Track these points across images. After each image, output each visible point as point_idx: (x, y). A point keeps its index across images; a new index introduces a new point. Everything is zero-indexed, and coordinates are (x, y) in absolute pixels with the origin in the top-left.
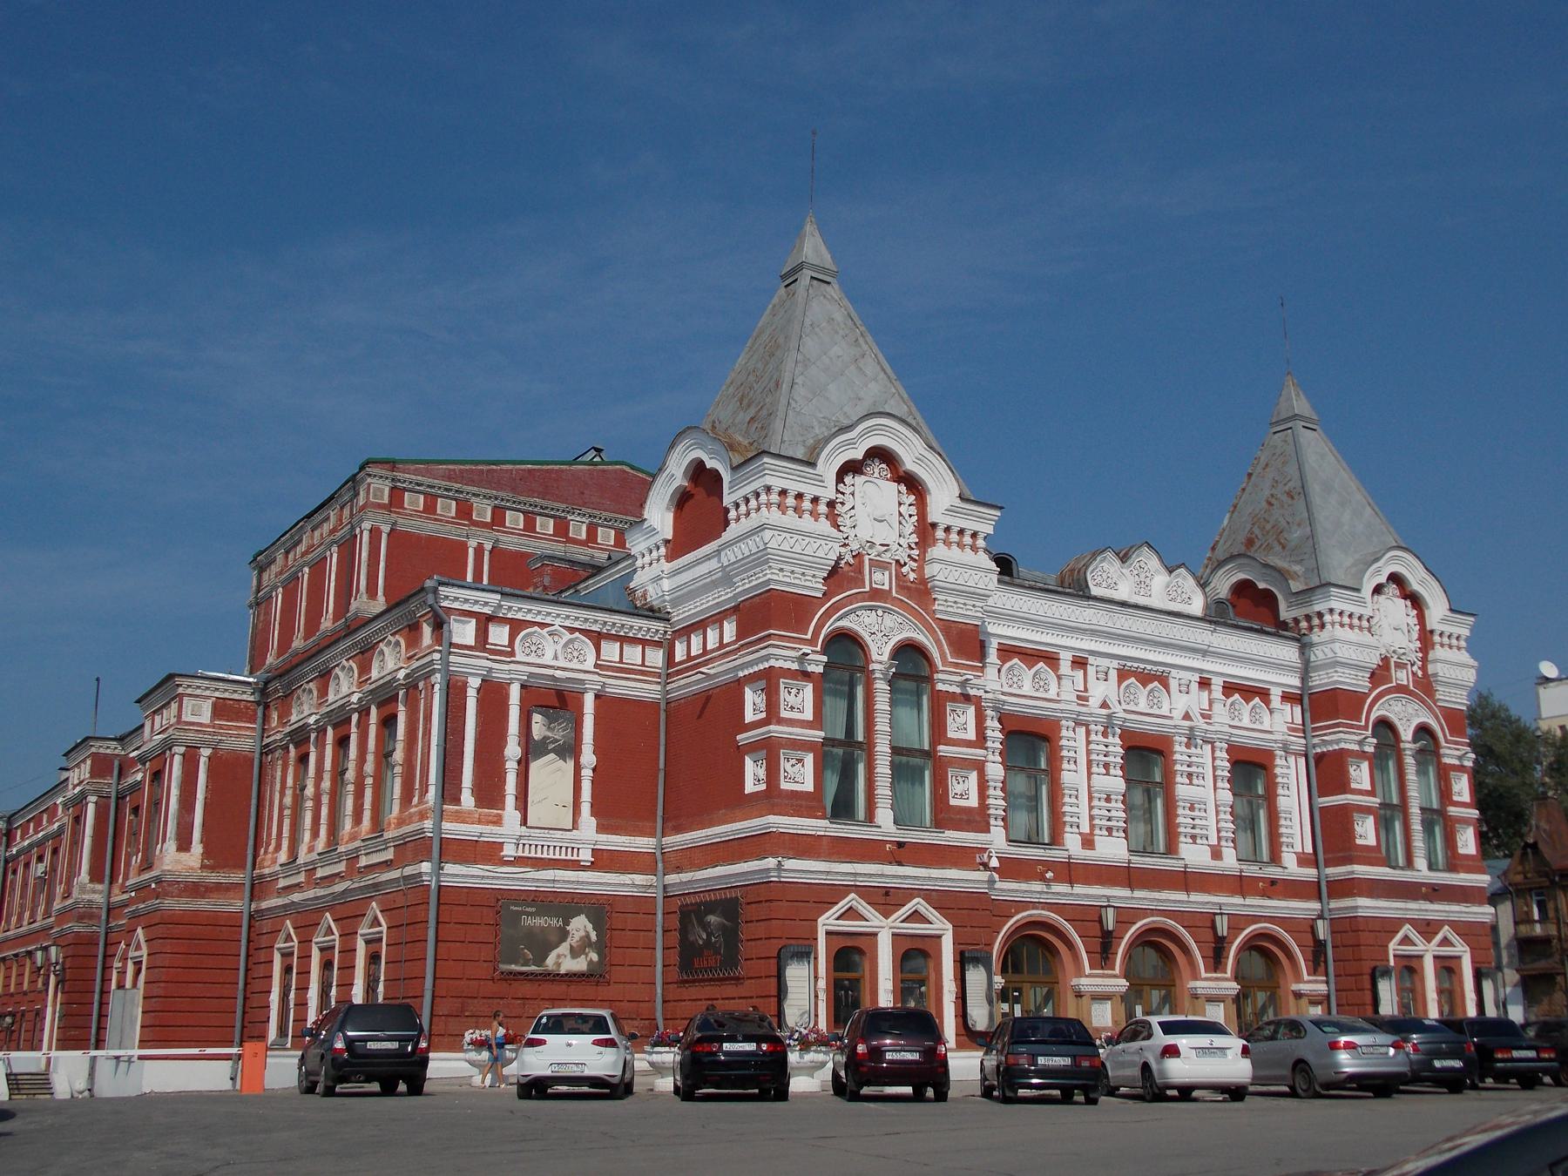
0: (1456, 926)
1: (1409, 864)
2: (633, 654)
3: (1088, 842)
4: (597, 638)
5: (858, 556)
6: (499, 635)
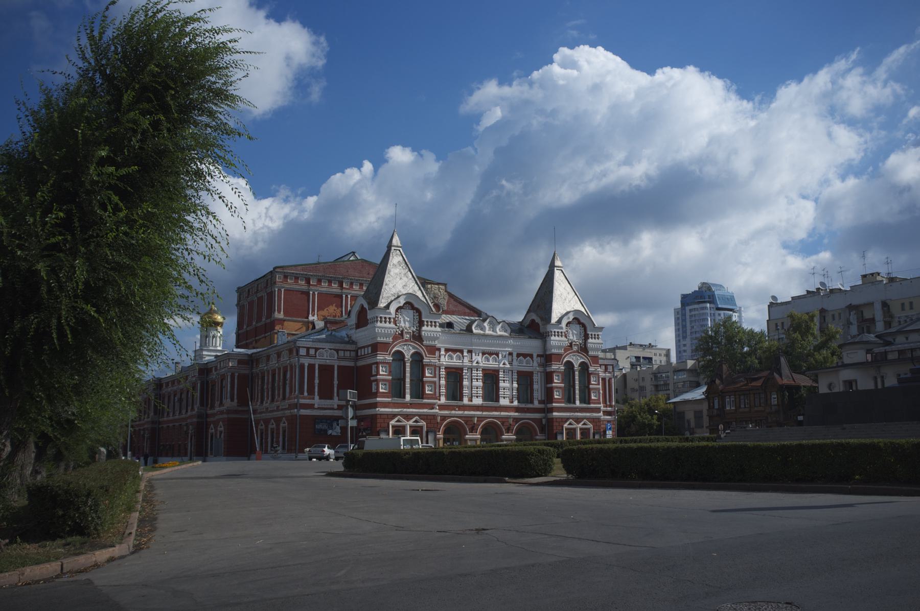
0: (588, 419)
1: (574, 403)
2: (347, 354)
4: (337, 351)
5: (402, 331)
6: (312, 352)
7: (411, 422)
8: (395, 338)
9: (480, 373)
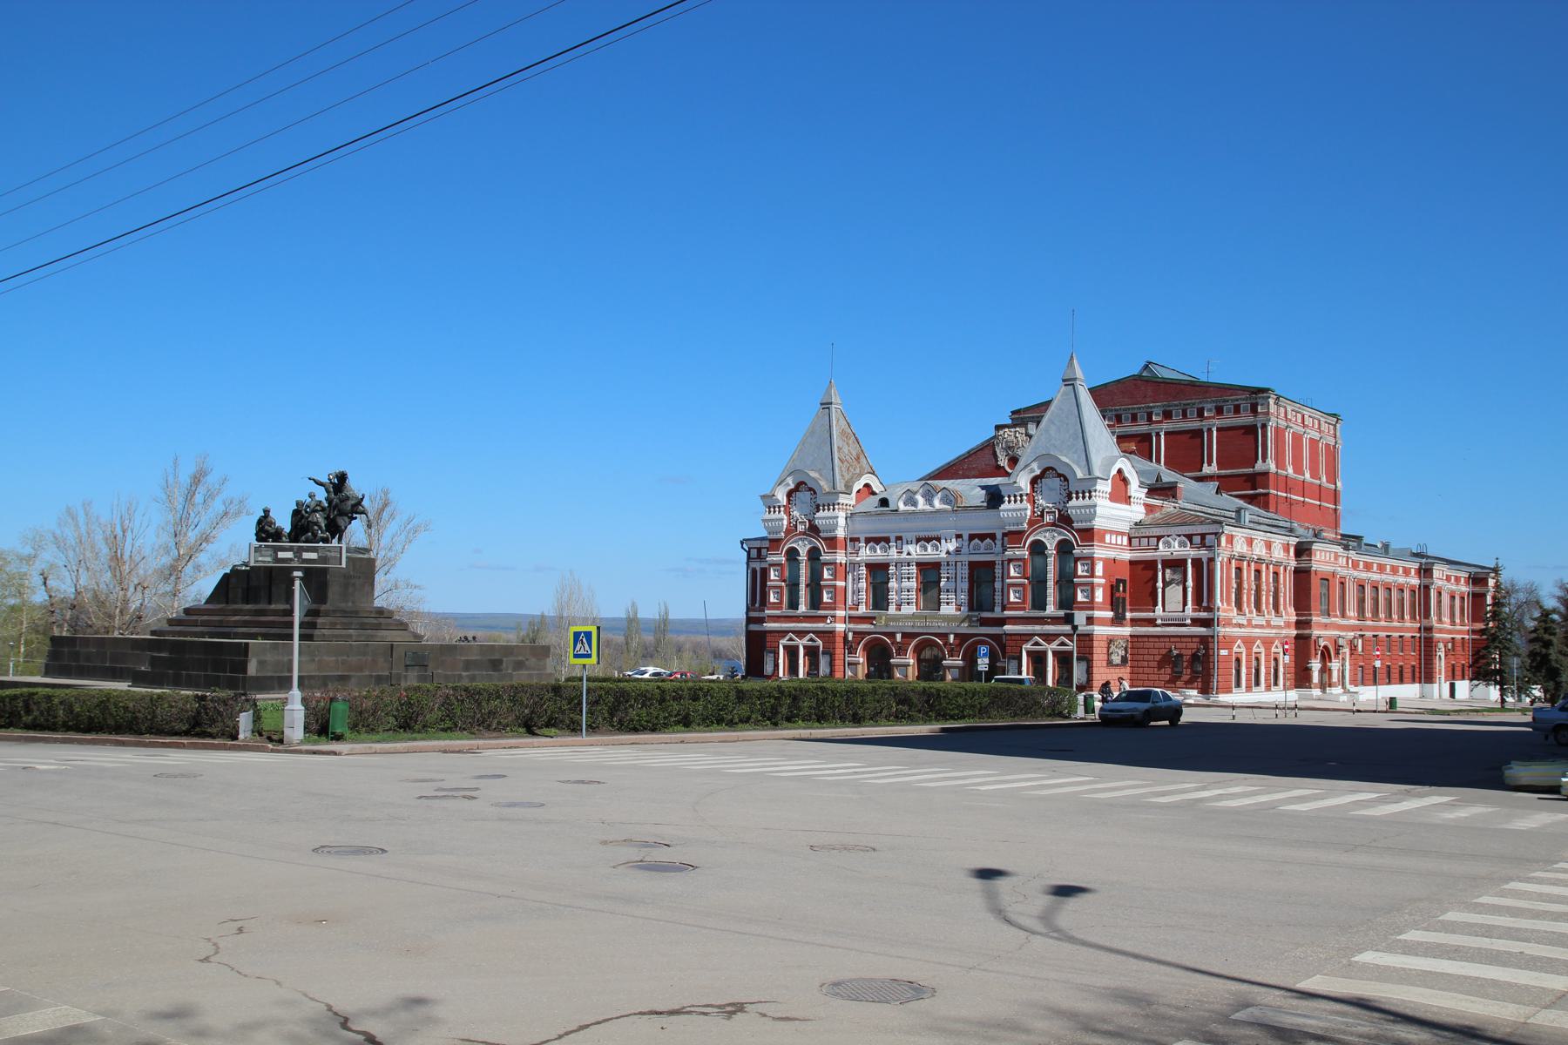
3: (899, 607)
7: (805, 641)
8: (788, 532)
9: (914, 569)
